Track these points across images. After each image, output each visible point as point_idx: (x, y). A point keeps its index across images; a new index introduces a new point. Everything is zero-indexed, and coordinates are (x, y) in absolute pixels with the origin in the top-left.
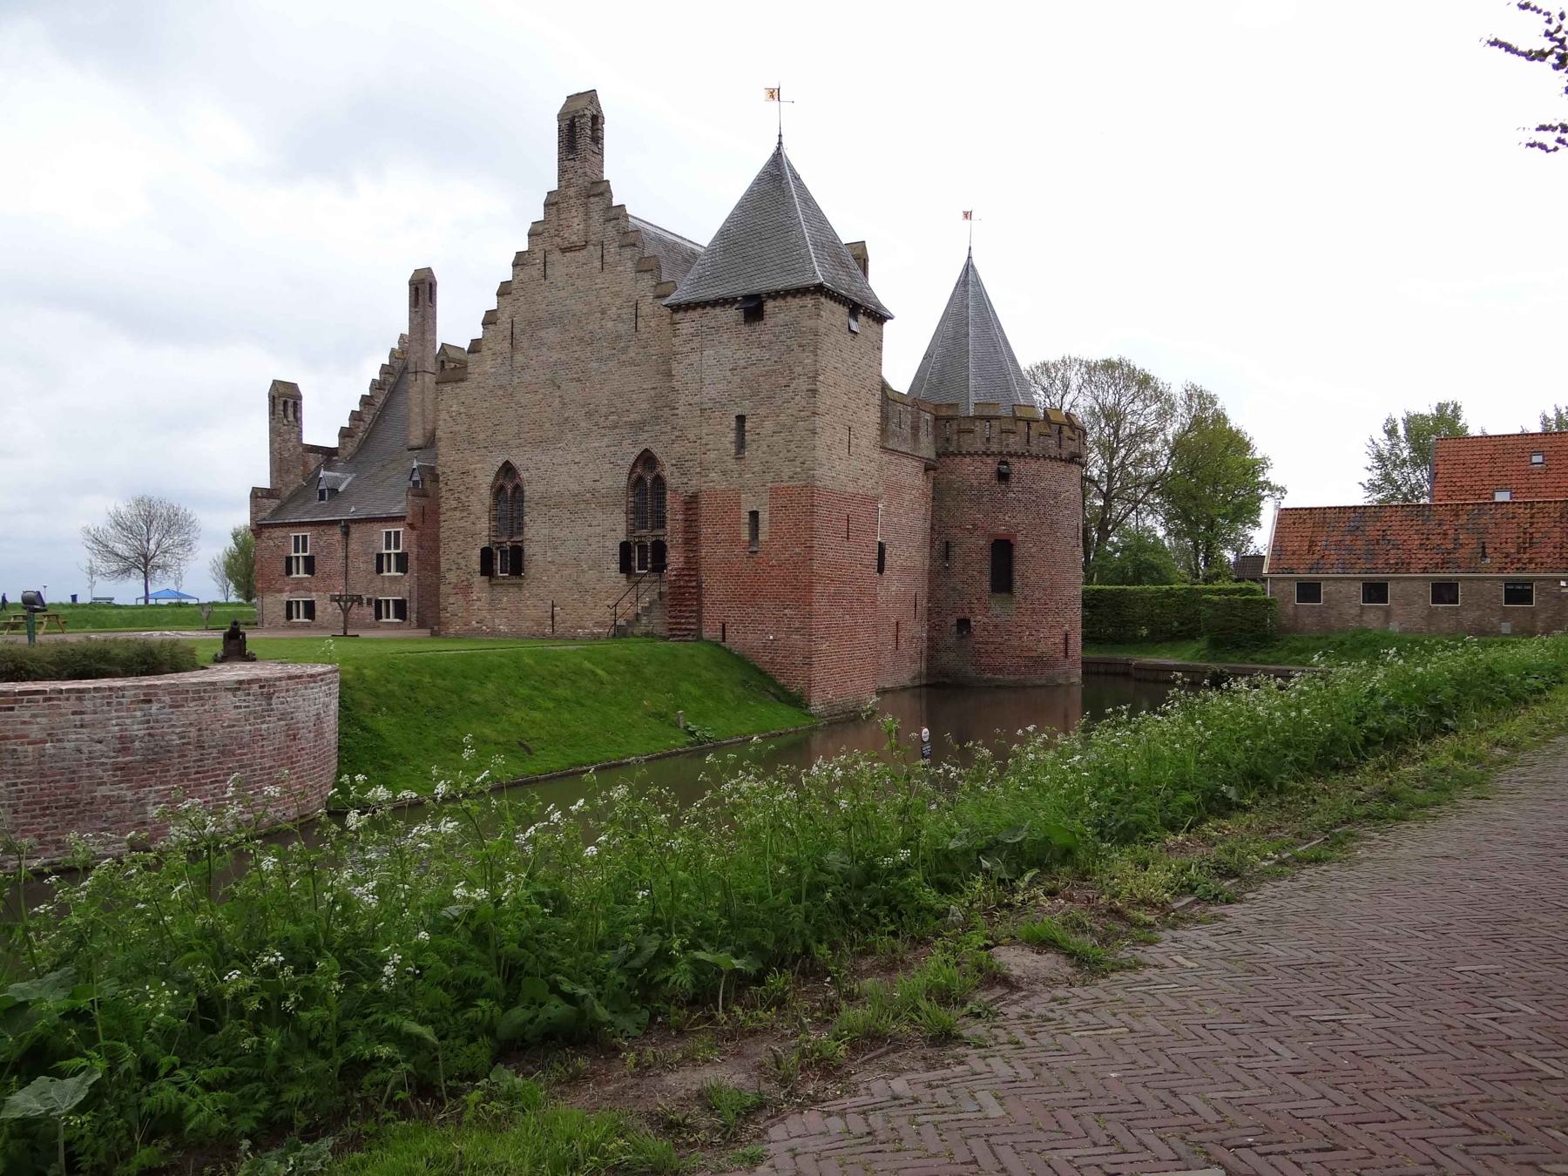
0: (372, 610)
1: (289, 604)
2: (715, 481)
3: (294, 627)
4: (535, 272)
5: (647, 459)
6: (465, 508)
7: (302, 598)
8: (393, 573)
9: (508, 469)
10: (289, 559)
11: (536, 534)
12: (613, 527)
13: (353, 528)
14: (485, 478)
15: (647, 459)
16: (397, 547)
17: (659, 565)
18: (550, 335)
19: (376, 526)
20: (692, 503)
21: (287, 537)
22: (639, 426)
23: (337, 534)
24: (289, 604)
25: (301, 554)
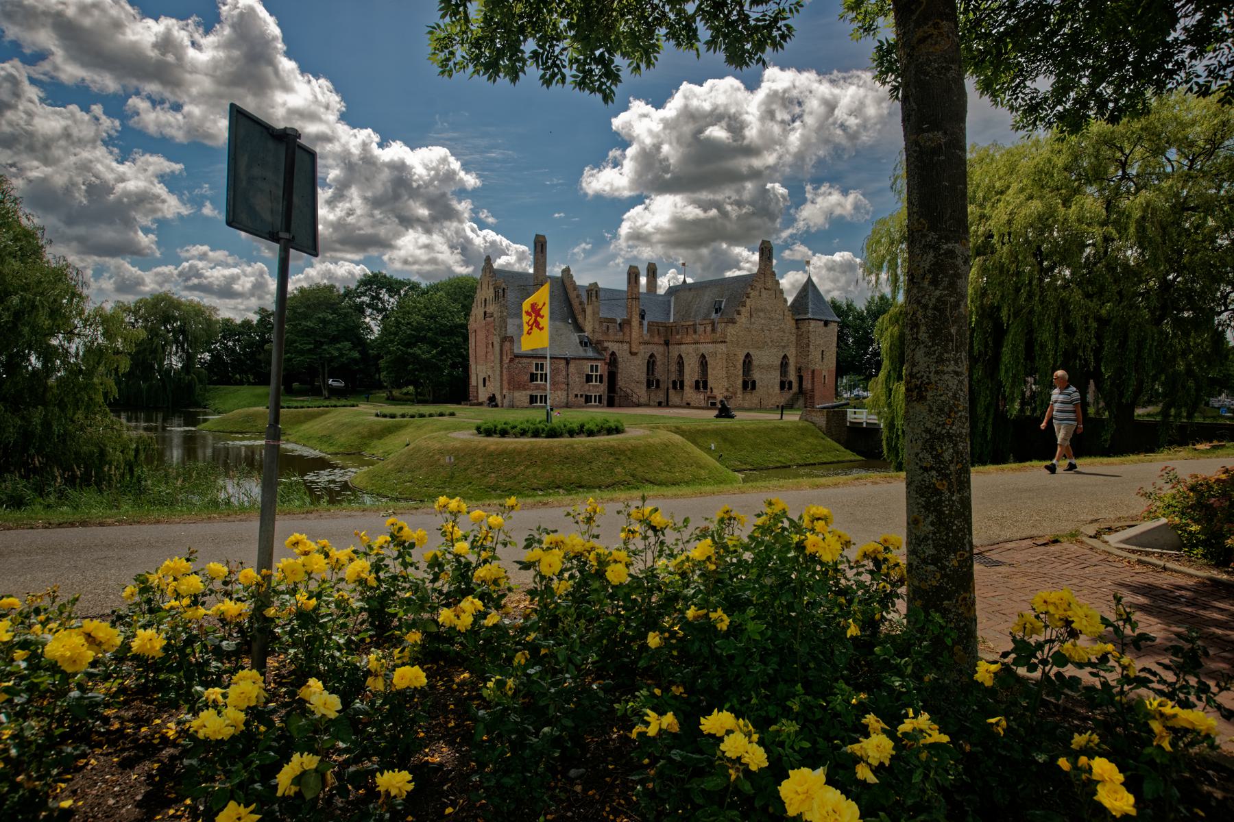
0: (583, 399)
1: (531, 396)
2: (817, 367)
3: (534, 407)
4: (758, 293)
5: (785, 357)
6: (735, 366)
7: (538, 393)
8: (594, 383)
9: (748, 355)
10: (532, 375)
11: (756, 375)
12: (776, 377)
13: (571, 362)
14: (741, 358)
15: (785, 357)
16: (597, 371)
17: (790, 388)
18: (762, 314)
19: (585, 362)
20: (813, 372)
21: (530, 363)
22: (784, 347)
23: (563, 363)
24: (531, 396)
25: (539, 372)
